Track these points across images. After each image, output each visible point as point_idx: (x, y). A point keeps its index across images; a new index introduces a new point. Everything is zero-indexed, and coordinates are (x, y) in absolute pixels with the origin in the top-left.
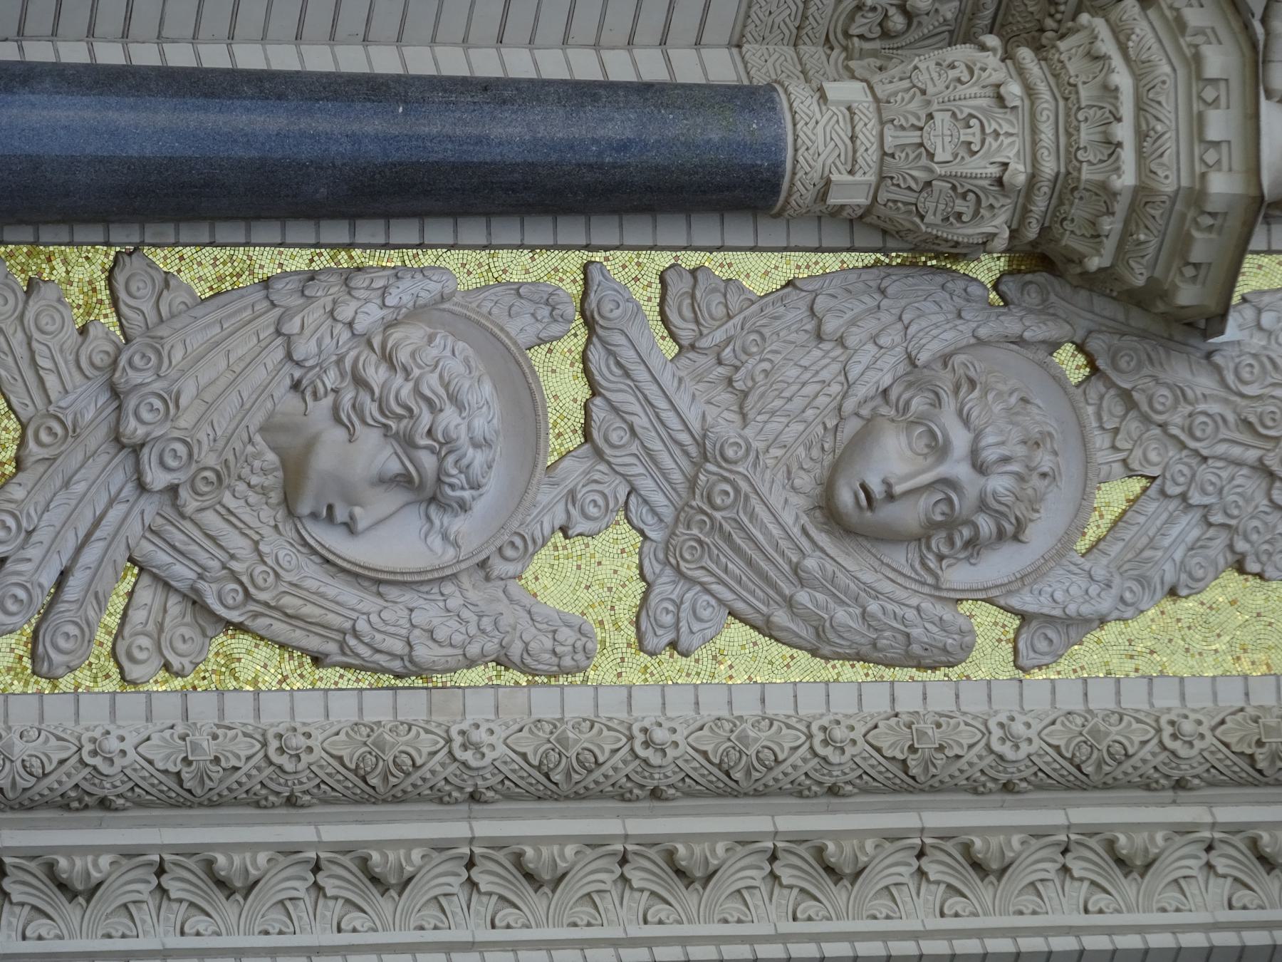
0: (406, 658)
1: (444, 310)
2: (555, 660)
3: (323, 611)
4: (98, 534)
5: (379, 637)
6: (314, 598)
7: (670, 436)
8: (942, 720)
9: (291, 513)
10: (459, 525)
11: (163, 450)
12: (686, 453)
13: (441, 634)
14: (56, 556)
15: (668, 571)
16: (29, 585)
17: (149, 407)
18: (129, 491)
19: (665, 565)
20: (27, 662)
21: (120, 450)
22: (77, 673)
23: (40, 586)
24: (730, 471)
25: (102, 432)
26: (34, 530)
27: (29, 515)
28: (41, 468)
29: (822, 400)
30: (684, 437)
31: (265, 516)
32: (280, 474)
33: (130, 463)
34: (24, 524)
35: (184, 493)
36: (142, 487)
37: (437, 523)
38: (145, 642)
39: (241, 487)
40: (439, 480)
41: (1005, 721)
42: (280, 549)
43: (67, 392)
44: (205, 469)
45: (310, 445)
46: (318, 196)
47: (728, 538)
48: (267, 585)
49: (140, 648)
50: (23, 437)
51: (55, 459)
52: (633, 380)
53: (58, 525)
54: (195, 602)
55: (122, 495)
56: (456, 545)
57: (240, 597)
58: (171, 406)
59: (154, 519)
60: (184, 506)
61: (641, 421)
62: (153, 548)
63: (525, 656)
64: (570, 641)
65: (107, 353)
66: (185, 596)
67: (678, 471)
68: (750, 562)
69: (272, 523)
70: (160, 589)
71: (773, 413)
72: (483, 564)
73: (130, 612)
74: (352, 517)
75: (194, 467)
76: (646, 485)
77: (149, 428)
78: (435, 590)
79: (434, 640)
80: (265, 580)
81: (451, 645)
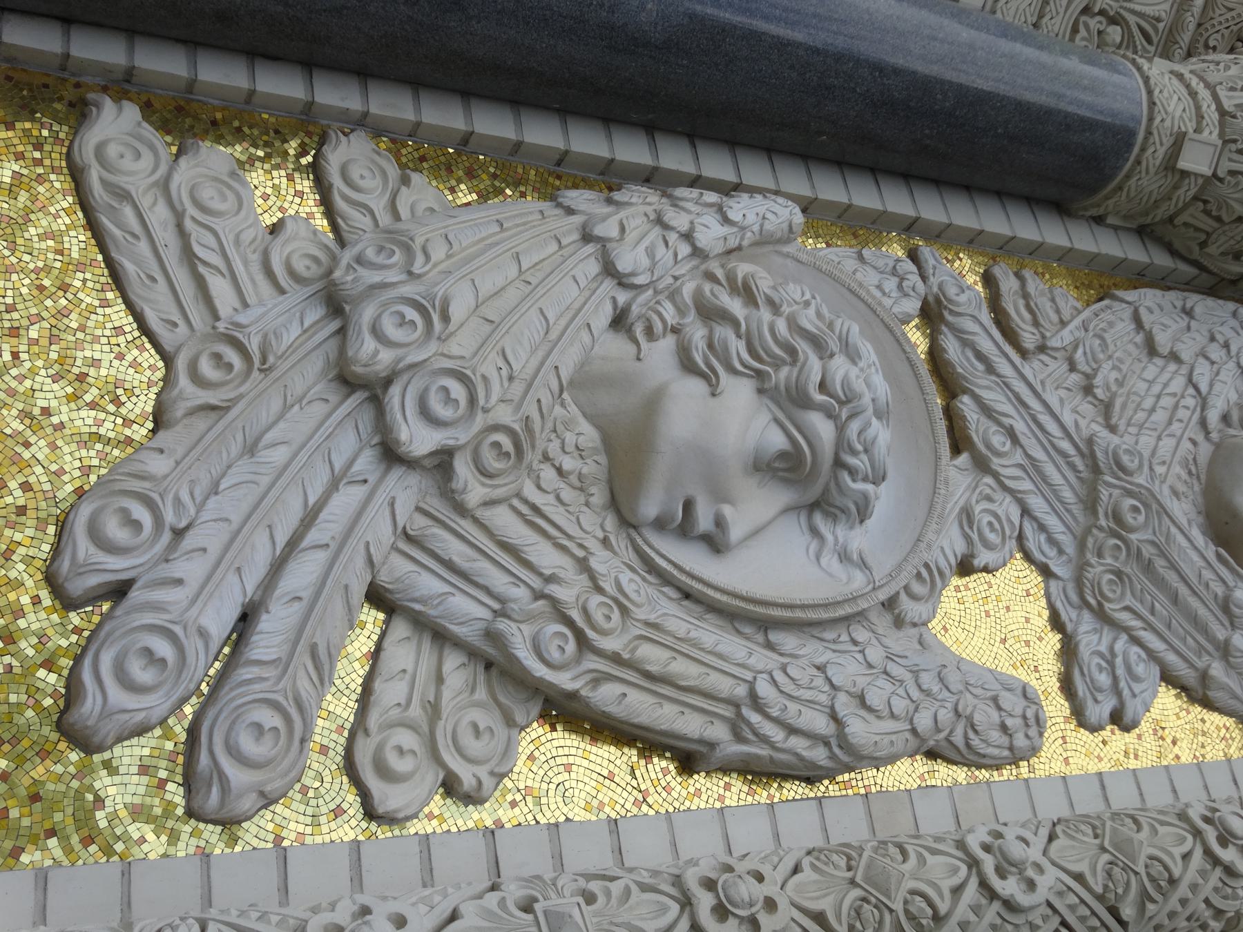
0: (833, 742)
1: (787, 255)
2: (1004, 740)
3: (704, 670)
4: (313, 536)
5: (793, 707)
6: (685, 648)
7: (1050, 441)
8: (595, 886)
9: (627, 523)
10: (859, 539)
11: (426, 390)
12: (1072, 466)
13: (874, 699)
14: (232, 578)
15: (1086, 615)
16: (177, 629)
17: (397, 320)
18: (366, 463)
19: (1080, 608)
20: (175, 793)
21: (348, 396)
22: (278, 808)
23: (203, 634)
24: (1131, 483)
25: (316, 365)
26: (187, 528)
27: (178, 501)
28: (201, 423)
29: (1182, 414)
30: (1065, 445)
31: (590, 522)
32: (603, 459)
33: (366, 418)
34: (169, 517)
35: (462, 468)
36: (391, 455)
37: (829, 538)
38: (406, 739)
39: (548, 474)
40: (838, 463)
41: (988, 839)
42: (614, 567)
43: (246, 305)
44: (496, 428)
45: (653, 404)
46: (643, 17)
47: (1148, 568)
48: (611, 625)
49: (401, 751)
50: (168, 380)
51: (228, 409)
52: (999, 376)
53: (236, 519)
54: (495, 664)
55: (357, 467)
56: (864, 565)
57: (571, 647)
58: (436, 318)
59: (410, 518)
60: (464, 491)
61: (1020, 427)
62: (411, 567)
63: (971, 735)
64: (1018, 711)
65: (316, 260)
66: (472, 653)
67: (1067, 488)
68: (1175, 599)
69: (601, 535)
70: (427, 644)
71: (1141, 427)
72: (890, 604)
73: (378, 685)
74: (720, 522)
75: (480, 421)
76: (1037, 503)
77: (400, 352)
78: (845, 637)
79: (870, 709)
80: (608, 618)
81: (893, 716)
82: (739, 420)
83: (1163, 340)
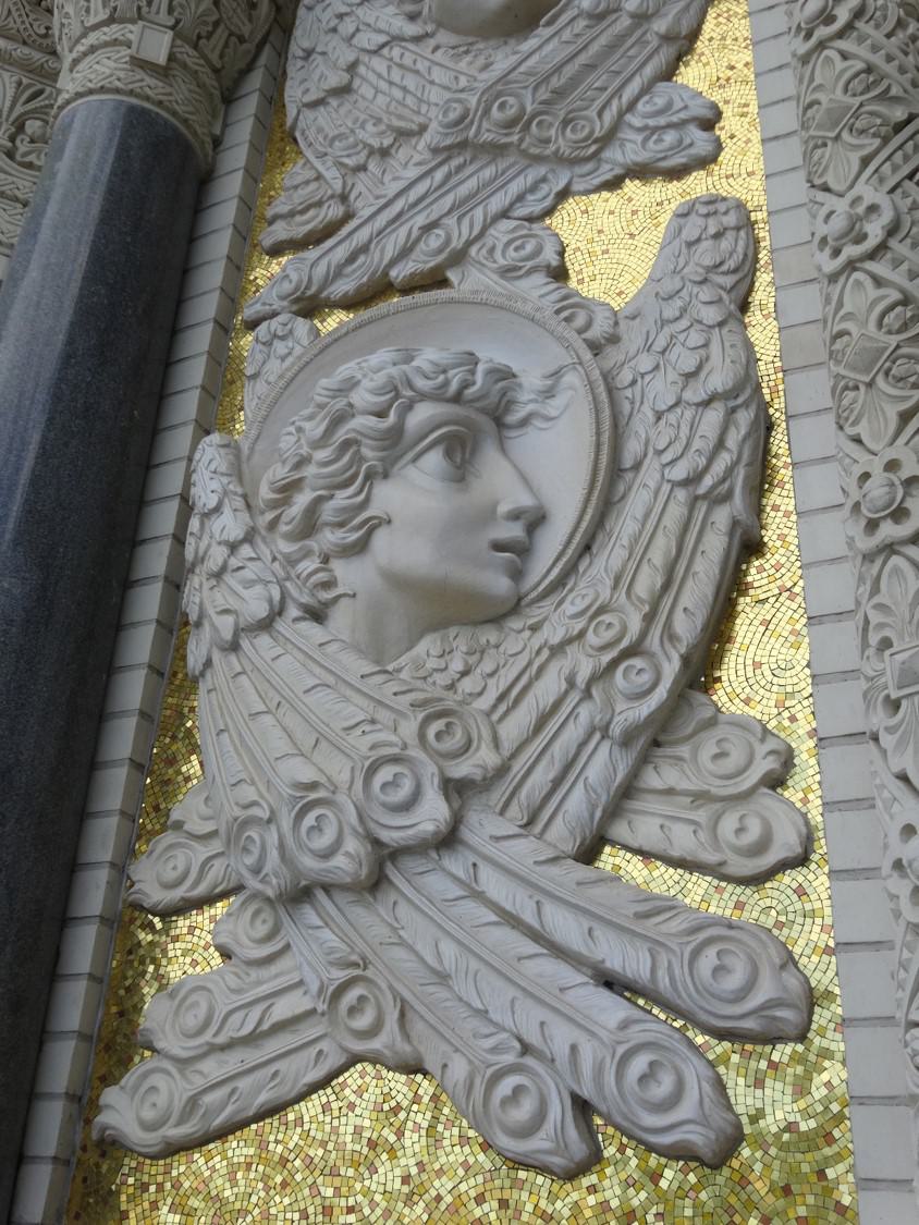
0: (732, 404)
1: (252, 449)
2: (730, 235)
3: (660, 531)
4: (529, 917)
5: (697, 444)
6: (639, 550)
7: (436, 190)
8: (874, 639)
9: (516, 607)
10: (531, 379)
11: (384, 805)
12: (459, 169)
13: (689, 363)
14: (570, 996)
15: (607, 154)
16: (621, 1050)
17: (315, 834)
18: (456, 864)
19: (600, 160)
20: (782, 1052)
21: (391, 882)
22: (797, 950)
23: (625, 1025)
24: (477, 110)
25: (359, 914)
26: (520, 1040)
27: (494, 1050)
28: (417, 1027)
29: (408, 60)
30: (439, 175)
31: (516, 644)
32: (453, 631)
33: (412, 864)
34: (509, 1058)
35: (461, 769)
36: (448, 840)
37: (531, 407)
38: (729, 824)
39: (467, 685)
40: (457, 398)
41: (828, 251)
43: (301, 983)
44: (422, 736)
45: (399, 582)
46: (16, 591)
47: (559, 94)
48: (616, 622)
49: (740, 830)
50: (374, 1059)
51: (403, 1001)
52: (370, 241)
53: (512, 992)
54: (654, 738)
55: (461, 874)
56: (556, 374)
57: (637, 662)
58: (313, 796)
59: (510, 820)
60: (485, 768)
62: (559, 819)
63: (725, 268)
64: (701, 222)
65: (256, 913)
66: (644, 760)
67: (481, 174)
68: (590, 67)
69: (527, 633)
70: (635, 804)
71: (421, 100)
72: (596, 348)
73: (676, 853)
74: (515, 516)
75: (415, 752)
76: (497, 203)
77: (347, 830)
78: (628, 393)
79: (699, 368)
81: (706, 345)
82: (414, 496)
83: (335, 79)
